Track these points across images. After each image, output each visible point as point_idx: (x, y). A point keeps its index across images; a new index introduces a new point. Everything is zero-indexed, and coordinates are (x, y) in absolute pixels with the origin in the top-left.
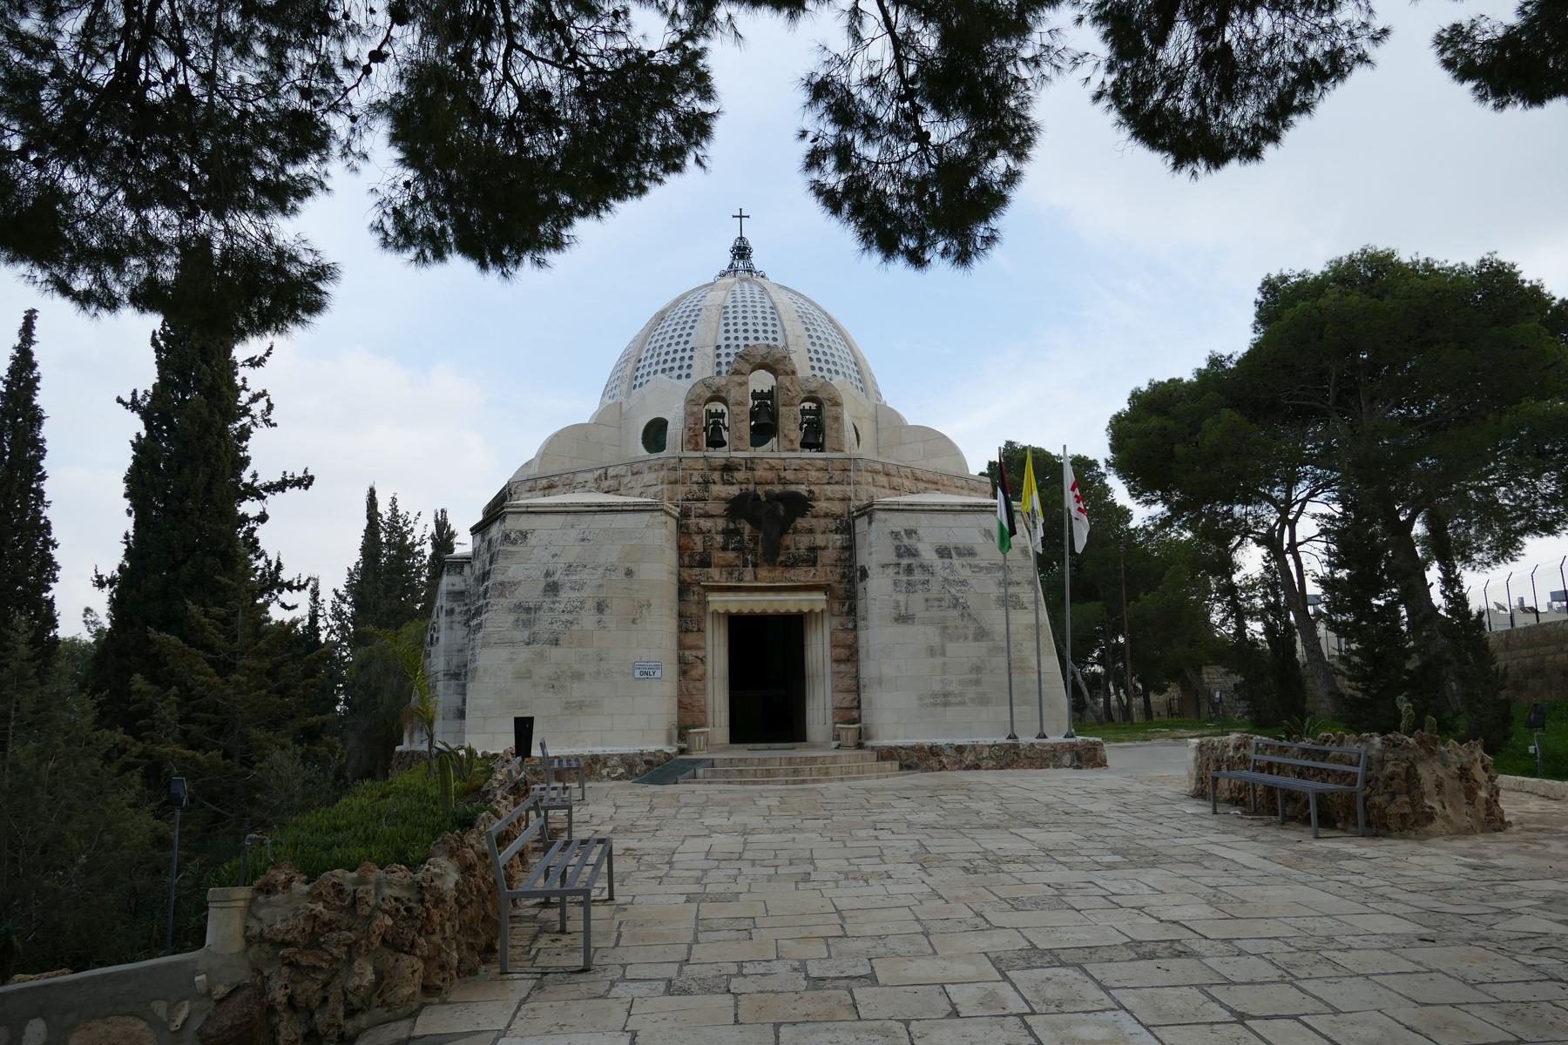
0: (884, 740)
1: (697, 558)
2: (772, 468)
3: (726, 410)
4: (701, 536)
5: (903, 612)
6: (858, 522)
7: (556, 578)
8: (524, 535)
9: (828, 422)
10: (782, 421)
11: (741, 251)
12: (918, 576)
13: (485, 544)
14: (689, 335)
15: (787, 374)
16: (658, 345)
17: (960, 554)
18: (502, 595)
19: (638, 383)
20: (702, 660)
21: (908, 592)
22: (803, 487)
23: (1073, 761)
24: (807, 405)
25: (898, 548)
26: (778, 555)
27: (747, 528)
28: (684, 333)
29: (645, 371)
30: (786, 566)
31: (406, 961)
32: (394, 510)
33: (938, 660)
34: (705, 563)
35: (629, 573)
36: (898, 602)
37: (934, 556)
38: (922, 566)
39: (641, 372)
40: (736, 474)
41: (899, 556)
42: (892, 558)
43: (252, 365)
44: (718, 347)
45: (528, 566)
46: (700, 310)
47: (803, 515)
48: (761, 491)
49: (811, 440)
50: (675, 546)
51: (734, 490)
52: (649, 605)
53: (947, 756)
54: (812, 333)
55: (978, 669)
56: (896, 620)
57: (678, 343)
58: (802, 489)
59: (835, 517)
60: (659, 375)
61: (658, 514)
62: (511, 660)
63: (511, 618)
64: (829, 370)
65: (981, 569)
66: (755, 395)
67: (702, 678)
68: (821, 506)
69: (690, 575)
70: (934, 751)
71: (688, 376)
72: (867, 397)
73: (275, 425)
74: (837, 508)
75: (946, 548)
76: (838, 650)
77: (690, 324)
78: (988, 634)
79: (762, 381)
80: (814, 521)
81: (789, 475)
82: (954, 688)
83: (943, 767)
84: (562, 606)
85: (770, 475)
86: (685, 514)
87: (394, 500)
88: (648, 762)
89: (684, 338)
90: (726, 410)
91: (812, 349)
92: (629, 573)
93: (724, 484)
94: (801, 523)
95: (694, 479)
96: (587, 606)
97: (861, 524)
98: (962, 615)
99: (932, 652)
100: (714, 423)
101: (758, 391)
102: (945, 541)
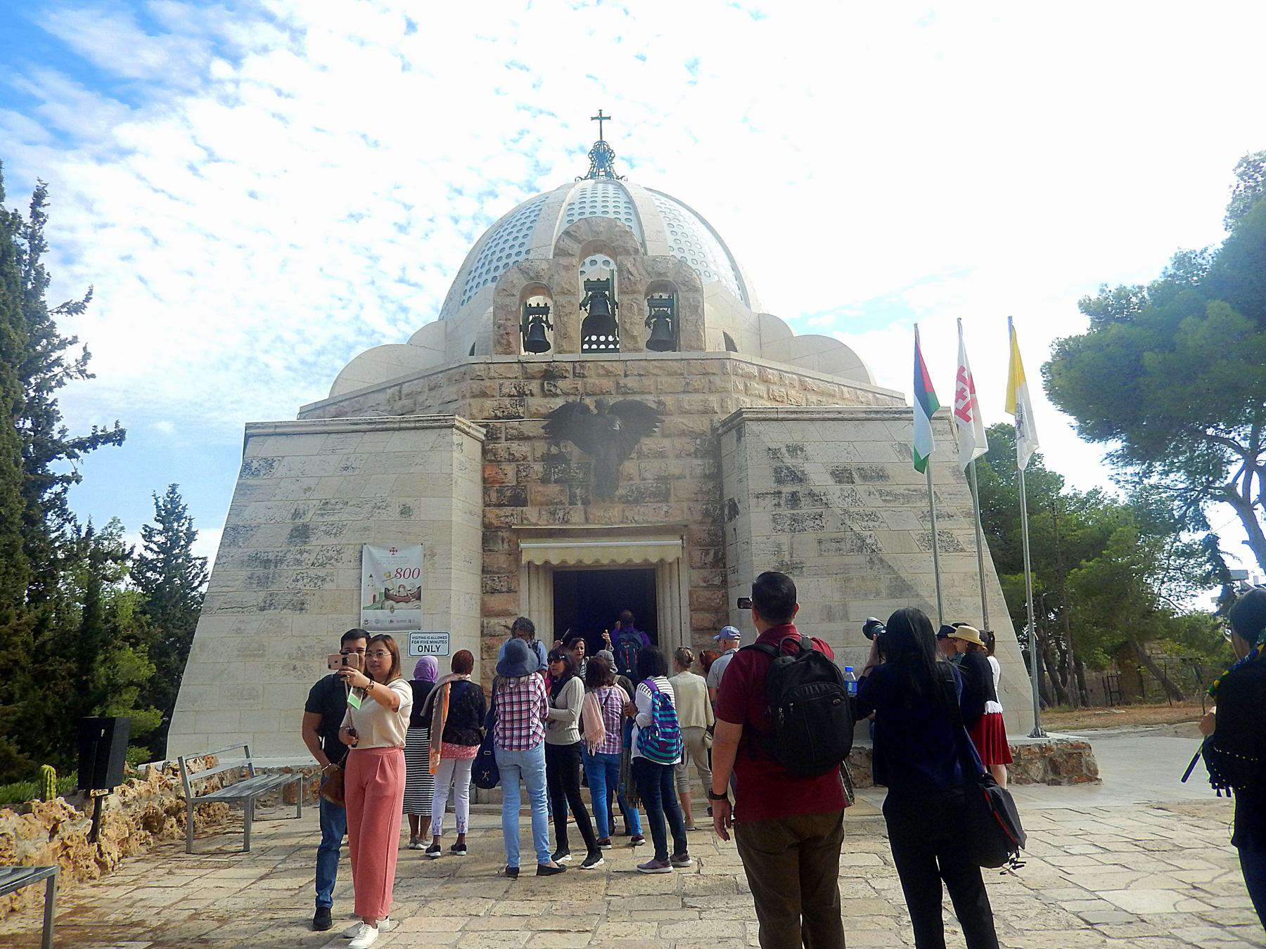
1: (508, 493)
2: (608, 374)
5: (787, 559)
6: (724, 440)
7: (305, 520)
9: (684, 313)
11: (601, 156)
12: (806, 508)
15: (628, 253)
17: (864, 478)
19: (466, 298)
22: (651, 397)
23: (1046, 772)
24: (656, 296)
25: (777, 471)
28: (521, 235)
29: (474, 284)
30: (628, 502)
34: (518, 500)
35: (406, 511)
36: (779, 545)
37: (831, 481)
38: (811, 494)
39: (470, 284)
40: (560, 383)
41: (779, 481)
42: (771, 485)
43: (69, 312)
45: (270, 504)
47: (649, 433)
49: (663, 337)
50: (478, 477)
51: (558, 403)
58: (650, 401)
59: (694, 435)
62: (238, 631)
63: (245, 573)
65: (896, 497)
66: (589, 285)
68: (676, 421)
69: (498, 517)
73: (93, 376)
74: (701, 424)
76: (700, 616)
79: (600, 268)
80: (667, 443)
81: (631, 382)
85: (607, 384)
86: (492, 436)
92: (406, 511)
93: (545, 396)
94: (648, 444)
95: (505, 390)
97: (729, 442)
98: (871, 561)
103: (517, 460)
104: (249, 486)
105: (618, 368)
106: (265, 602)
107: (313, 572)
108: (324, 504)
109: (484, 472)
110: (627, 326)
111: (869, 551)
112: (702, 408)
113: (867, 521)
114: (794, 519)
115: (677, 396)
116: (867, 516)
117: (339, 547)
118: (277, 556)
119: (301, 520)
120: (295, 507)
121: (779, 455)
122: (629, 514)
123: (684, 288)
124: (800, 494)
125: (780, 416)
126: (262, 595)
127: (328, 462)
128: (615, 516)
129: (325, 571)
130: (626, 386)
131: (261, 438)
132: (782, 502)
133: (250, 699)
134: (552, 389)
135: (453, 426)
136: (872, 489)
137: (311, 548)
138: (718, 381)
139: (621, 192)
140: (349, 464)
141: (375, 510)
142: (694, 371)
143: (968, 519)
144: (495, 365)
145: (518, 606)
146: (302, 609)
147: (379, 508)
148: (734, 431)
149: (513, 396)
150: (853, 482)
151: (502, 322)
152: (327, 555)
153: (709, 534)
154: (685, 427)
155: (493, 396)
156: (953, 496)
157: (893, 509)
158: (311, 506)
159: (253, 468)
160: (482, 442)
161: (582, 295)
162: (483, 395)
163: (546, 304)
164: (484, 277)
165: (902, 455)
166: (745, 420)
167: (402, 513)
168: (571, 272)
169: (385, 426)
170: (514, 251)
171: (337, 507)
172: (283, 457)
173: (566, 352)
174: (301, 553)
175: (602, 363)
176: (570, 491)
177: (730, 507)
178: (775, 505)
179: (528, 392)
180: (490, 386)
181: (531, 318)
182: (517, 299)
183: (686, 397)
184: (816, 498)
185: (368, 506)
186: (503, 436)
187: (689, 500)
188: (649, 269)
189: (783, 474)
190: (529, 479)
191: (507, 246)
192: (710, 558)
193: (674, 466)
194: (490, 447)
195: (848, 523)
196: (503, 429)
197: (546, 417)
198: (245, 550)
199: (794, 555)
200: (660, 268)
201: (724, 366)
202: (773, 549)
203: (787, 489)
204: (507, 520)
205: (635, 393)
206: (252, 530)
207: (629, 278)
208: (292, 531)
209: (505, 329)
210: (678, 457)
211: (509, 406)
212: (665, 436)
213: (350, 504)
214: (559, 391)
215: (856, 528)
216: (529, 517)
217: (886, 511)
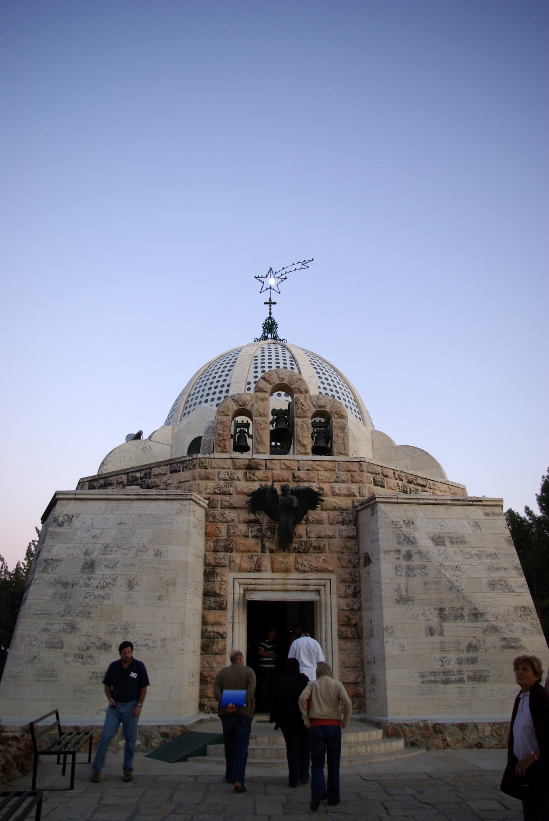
1: (222, 544)
2: (288, 468)
4: (226, 525)
5: (404, 593)
6: (361, 514)
7: (94, 556)
8: (70, 518)
9: (336, 432)
10: (297, 430)
12: (416, 561)
14: (227, 375)
15: (301, 392)
16: (203, 384)
18: (45, 570)
19: (186, 411)
20: (223, 636)
21: (408, 576)
22: (314, 485)
24: (317, 419)
26: (292, 542)
27: (265, 519)
28: (224, 374)
29: (193, 403)
30: (299, 552)
33: (436, 639)
35: (158, 554)
36: (399, 585)
37: (431, 544)
39: (190, 403)
45: (70, 545)
46: (236, 359)
47: (314, 508)
48: (277, 486)
51: (256, 486)
52: (174, 584)
53: (451, 734)
54: (321, 375)
56: (398, 601)
57: (218, 381)
58: (314, 486)
59: (342, 510)
60: (203, 404)
61: (188, 502)
62: (46, 630)
63: (51, 591)
68: (330, 500)
74: (346, 503)
75: (440, 538)
77: (228, 368)
80: (324, 514)
81: (302, 474)
82: (453, 666)
84: (96, 583)
85: (287, 475)
86: (212, 505)
88: (165, 735)
89: (224, 378)
91: (322, 386)
92: (158, 554)
93: (247, 480)
94: (312, 515)
95: (222, 476)
96: (119, 582)
97: (364, 516)
99: (431, 632)
100: (240, 431)
102: (438, 531)
103: (228, 522)
104: (56, 533)
105: (295, 465)
106: (65, 611)
107: (97, 592)
108: (105, 547)
109: (206, 529)
110: (301, 438)
111: (456, 591)
112: (346, 493)
113: (455, 571)
114: (408, 568)
115: (331, 484)
116: (454, 568)
117: (114, 576)
118: (73, 580)
119: (90, 557)
120: (86, 548)
121: (398, 526)
122: (300, 561)
123: (336, 416)
124: (412, 553)
125: (400, 501)
126: (63, 606)
127: (109, 519)
128: (290, 561)
129: (105, 592)
130: (299, 477)
131: (66, 502)
132: (401, 557)
133: (51, 677)
134: (252, 476)
135: (190, 499)
136: (457, 550)
137: (96, 576)
139: (286, 350)
140: (122, 521)
141: (139, 552)
142: (342, 469)
143: (516, 571)
144: (216, 460)
145: (226, 619)
146: (89, 617)
147: (141, 551)
148: (369, 510)
149: (226, 480)
150: (445, 545)
151: (221, 432)
152: (106, 581)
153: (351, 575)
154: (336, 505)
155: (214, 480)
156: (506, 556)
157: (470, 563)
158: (97, 548)
159: (60, 521)
160: (206, 509)
162: (207, 478)
163: (247, 422)
164: (199, 399)
165: (475, 528)
166: (377, 502)
167: (156, 555)
168: (265, 403)
169: (146, 497)
170: (219, 384)
171: (114, 549)
172: (79, 514)
173: (261, 453)
174: (89, 579)
175: (284, 461)
176: (262, 544)
177: (365, 558)
178: (396, 559)
179: (236, 478)
180: (212, 473)
181: (238, 430)
182: (230, 418)
183: (336, 485)
184: (422, 555)
185: (134, 549)
186: (219, 505)
187: (338, 552)
188: (315, 403)
189: (401, 539)
190: (235, 535)
191: (215, 381)
192: (350, 591)
193: (328, 530)
194: (211, 513)
195: (444, 572)
196: (219, 501)
197: (248, 495)
198: (53, 575)
199: (409, 592)
200: (322, 402)
202: (395, 587)
203: (404, 548)
204: (220, 561)
205: (304, 481)
206: (57, 562)
207: (301, 408)
208: (84, 564)
209: (223, 436)
210: (331, 524)
211: (223, 486)
212: (323, 509)
213: (122, 547)
214: (256, 478)
215: (448, 575)
216: (235, 560)
217: (466, 564)
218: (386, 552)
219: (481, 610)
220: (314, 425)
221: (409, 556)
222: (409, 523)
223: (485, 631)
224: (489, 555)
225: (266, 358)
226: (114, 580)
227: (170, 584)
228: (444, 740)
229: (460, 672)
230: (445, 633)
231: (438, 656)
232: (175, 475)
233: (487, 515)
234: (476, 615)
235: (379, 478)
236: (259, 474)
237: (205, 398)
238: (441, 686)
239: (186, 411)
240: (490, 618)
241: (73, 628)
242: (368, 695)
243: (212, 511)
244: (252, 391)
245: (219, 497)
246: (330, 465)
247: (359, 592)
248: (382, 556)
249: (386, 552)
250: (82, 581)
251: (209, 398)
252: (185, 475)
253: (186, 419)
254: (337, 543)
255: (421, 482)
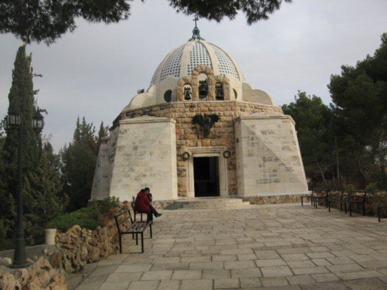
0: (246, 195)
2: (206, 106)
3: (191, 88)
8: (126, 131)
9: (225, 91)
12: (255, 141)
13: (114, 134)
14: (179, 61)
17: (269, 133)
18: (119, 150)
19: (162, 78)
20: (185, 170)
21: (252, 146)
24: (218, 85)
25: (249, 132)
27: (198, 126)
31: (95, 248)
32: (84, 122)
33: (262, 168)
35: (160, 142)
37: (261, 134)
41: (249, 134)
44: (189, 66)
47: (217, 121)
48: (203, 114)
49: (220, 95)
51: (194, 114)
52: (167, 153)
55: (274, 171)
56: (248, 155)
57: (175, 65)
58: (217, 113)
59: (228, 122)
62: (123, 171)
64: (226, 72)
66: (200, 82)
67: (185, 176)
68: (223, 118)
70: (261, 198)
71: (179, 76)
72: (239, 80)
74: (230, 119)
78: (278, 159)
79: (203, 77)
81: (212, 108)
82: (268, 177)
83: (264, 203)
85: (206, 109)
86: (177, 122)
87: (84, 119)
88: (168, 203)
90: (191, 88)
91: (220, 65)
92: (160, 142)
94: (217, 124)
97: (236, 124)
99: (260, 166)
101: (201, 80)
102: (264, 129)
105: (209, 105)
114: (253, 144)
126: (128, 163)
138: (234, 108)
148: (238, 122)
161: (198, 85)
162: (175, 112)
164: (167, 73)
170: (176, 66)
183: (226, 112)
193: (223, 130)
201: (235, 104)
203: (251, 136)
210: (224, 127)
212: (220, 122)
218: (245, 138)
219: (278, 157)
220: (216, 87)
221: (252, 139)
222: (253, 126)
223: (280, 165)
224: (283, 138)
225: (195, 52)
226: (145, 152)
227: (165, 153)
228: (263, 201)
229: (270, 179)
230: (266, 166)
231: (263, 174)
232: (162, 110)
233: (283, 122)
234: (277, 159)
235: (243, 108)
236: (195, 109)
237: (170, 72)
238: (264, 185)
239: (162, 78)
240: (282, 161)
241: (132, 170)
242: (238, 189)
243: (178, 124)
244: (191, 75)
245: (180, 119)
246: (224, 104)
247: (235, 152)
248: (243, 139)
249: (245, 138)
250: (133, 154)
251: (172, 73)
252: (166, 111)
253: (162, 82)
254: (226, 135)
255: (260, 107)
